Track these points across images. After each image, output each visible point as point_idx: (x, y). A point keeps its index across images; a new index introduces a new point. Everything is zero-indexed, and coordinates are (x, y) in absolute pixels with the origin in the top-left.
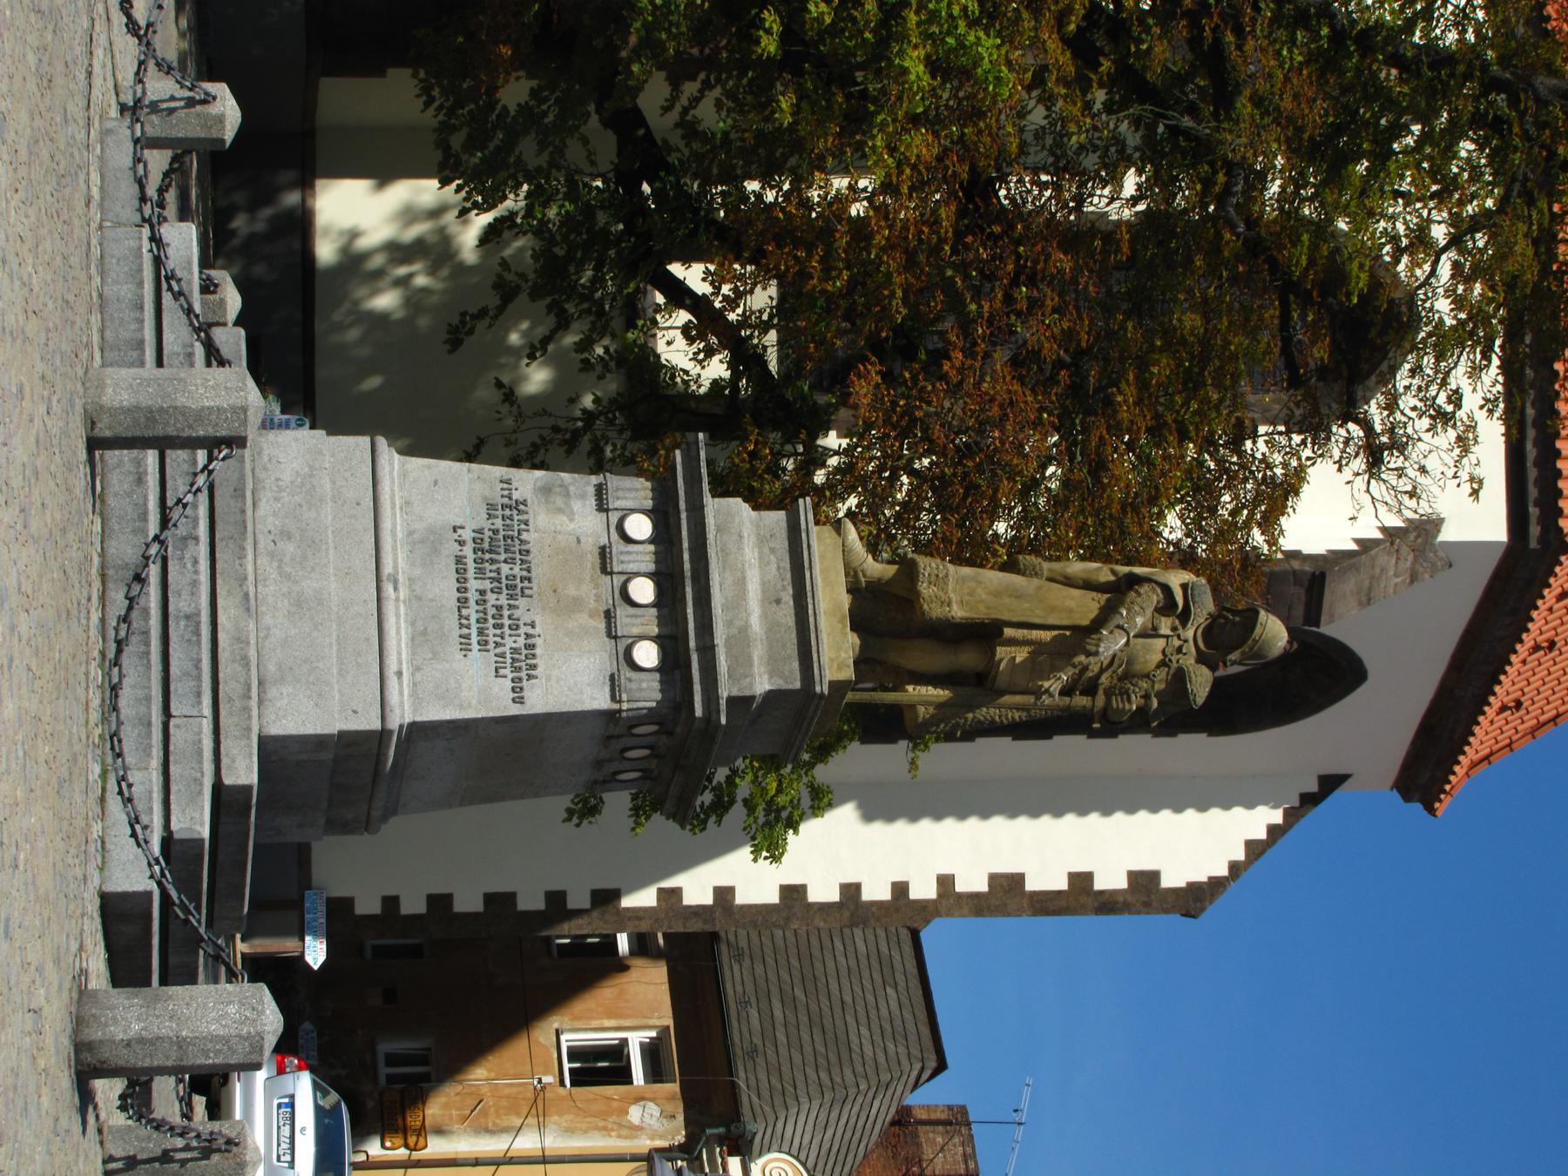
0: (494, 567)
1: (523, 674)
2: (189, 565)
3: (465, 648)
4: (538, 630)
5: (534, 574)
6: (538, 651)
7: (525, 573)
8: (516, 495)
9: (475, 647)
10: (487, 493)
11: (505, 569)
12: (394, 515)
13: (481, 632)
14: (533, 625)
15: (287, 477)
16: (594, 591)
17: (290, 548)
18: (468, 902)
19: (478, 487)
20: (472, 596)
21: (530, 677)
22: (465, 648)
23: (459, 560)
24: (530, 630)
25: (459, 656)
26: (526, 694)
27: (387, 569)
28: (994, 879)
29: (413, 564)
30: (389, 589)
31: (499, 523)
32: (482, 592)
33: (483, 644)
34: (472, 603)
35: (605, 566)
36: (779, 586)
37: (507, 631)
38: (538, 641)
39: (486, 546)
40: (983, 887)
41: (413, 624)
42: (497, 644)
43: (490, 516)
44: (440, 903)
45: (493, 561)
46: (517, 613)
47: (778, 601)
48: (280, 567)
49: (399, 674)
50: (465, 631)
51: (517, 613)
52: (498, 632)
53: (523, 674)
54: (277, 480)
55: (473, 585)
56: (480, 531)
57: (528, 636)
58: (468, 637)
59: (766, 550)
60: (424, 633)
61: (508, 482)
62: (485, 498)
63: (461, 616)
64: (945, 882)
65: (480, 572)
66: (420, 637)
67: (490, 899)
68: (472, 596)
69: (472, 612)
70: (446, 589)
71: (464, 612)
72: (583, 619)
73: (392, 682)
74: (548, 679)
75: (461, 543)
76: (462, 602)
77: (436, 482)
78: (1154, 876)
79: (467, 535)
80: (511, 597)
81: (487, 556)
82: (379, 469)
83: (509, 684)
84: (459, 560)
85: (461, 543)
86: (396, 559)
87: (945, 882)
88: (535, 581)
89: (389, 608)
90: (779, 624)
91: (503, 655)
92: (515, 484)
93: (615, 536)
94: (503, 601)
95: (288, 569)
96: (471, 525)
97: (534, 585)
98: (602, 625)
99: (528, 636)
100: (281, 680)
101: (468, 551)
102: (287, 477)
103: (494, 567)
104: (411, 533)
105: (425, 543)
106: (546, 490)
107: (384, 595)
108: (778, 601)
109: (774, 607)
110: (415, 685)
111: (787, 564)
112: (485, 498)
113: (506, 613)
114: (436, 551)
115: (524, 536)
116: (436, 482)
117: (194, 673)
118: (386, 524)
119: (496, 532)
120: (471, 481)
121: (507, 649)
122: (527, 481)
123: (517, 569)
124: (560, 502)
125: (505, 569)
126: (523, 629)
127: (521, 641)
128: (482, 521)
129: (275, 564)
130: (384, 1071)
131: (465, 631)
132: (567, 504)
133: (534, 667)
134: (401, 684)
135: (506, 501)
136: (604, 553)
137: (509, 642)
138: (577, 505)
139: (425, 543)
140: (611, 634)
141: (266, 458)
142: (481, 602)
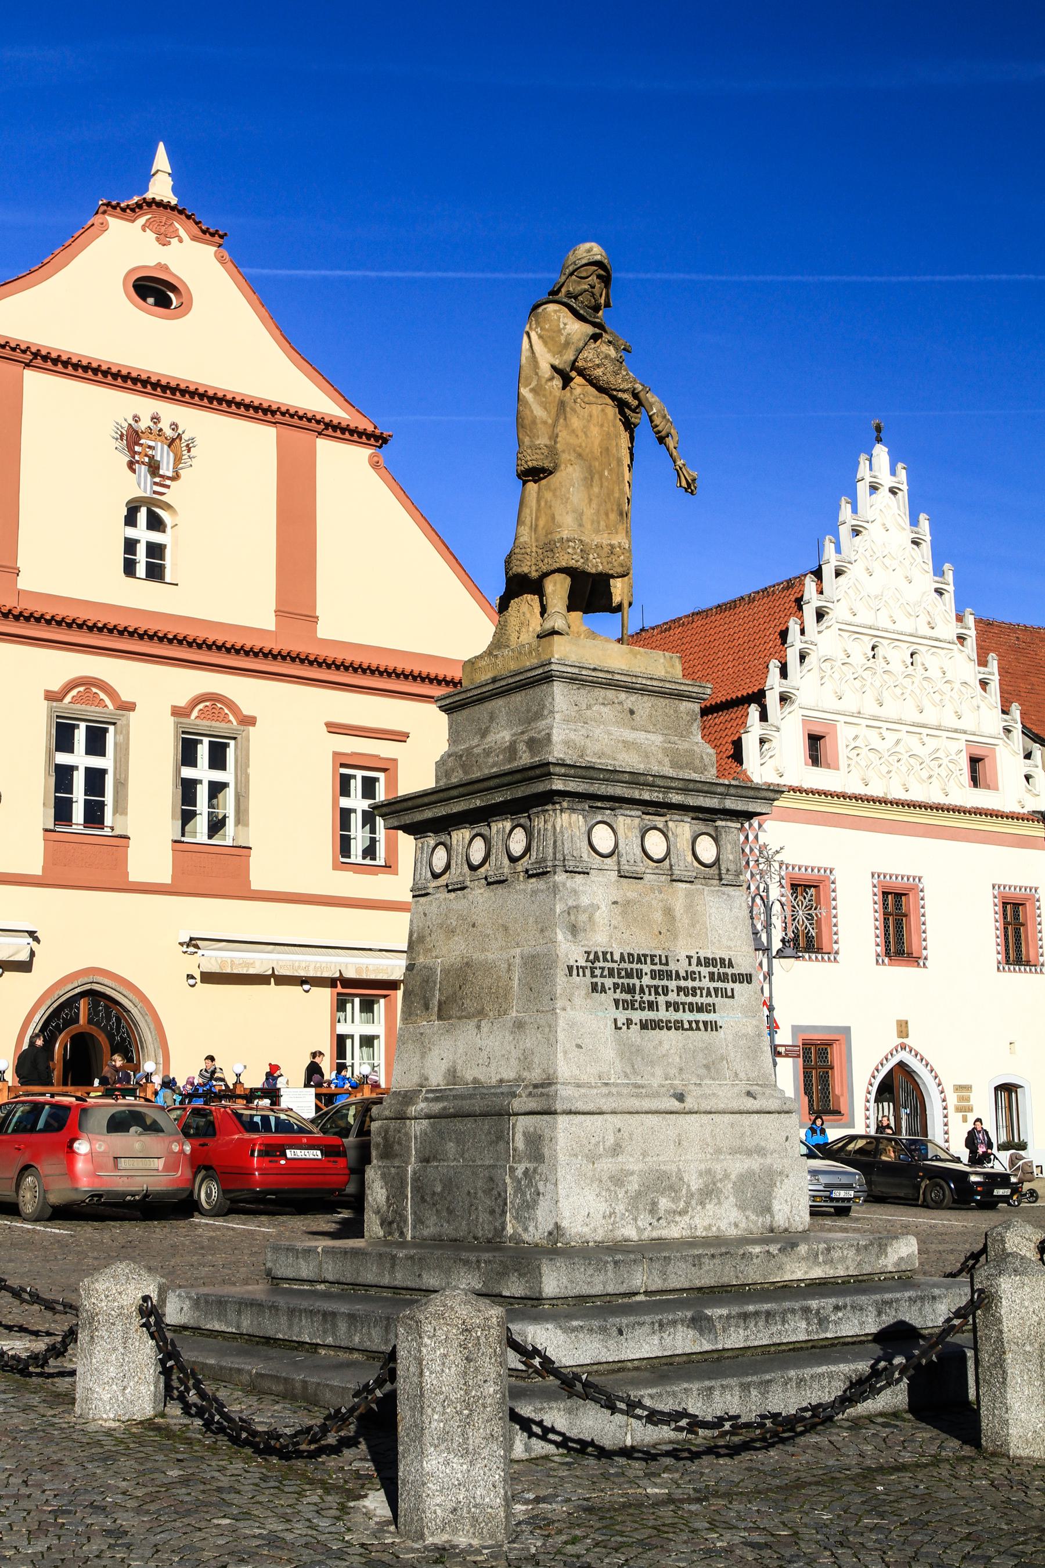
0: (647, 991)
1: (730, 971)
2: (840, 1314)
3: (714, 1026)
4: (693, 953)
11: (646, 980)
13: (700, 1009)
14: (689, 958)
16: (652, 892)
17: (664, 1203)
20: (673, 1016)
21: (731, 965)
22: (714, 1026)
23: (644, 1026)
24: (694, 961)
31: (609, 982)
32: (668, 1005)
33: (710, 1008)
36: (619, 708)
37: (696, 984)
38: (702, 955)
39: (629, 997)
42: (709, 994)
43: (604, 990)
45: (642, 991)
48: (680, 1214)
50: (701, 1025)
51: (682, 974)
53: (730, 971)
54: (604, 1217)
55: (662, 1014)
56: (616, 1002)
58: (705, 1023)
59: (589, 712)
60: (707, 1067)
61: (570, 968)
62: (587, 994)
63: (691, 1029)
65: (652, 1006)
68: (673, 1016)
69: (687, 1017)
71: (686, 1026)
72: (679, 907)
74: (730, 948)
75: (629, 1022)
76: (679, 1025)
77: (579, 1046)
79: (622, 1016)
80: (669, 976)
81: (637, 997)
83: (737, 986)
84: (644, 1026)
91: (716, 990)
92: (572, 963)
94: (672, 984)
95: (682, 1204)
97: (658, 952)
99: (699, 963)
100: (768, 1210)
101: (637, 1016)
102: (603, 1207)
103: (647, 991)
111: (600, 693)
114: (639, 1050)
115: (617, 957)
116: (579, 1046)
119: (616, 986)
121: (712, 985)
123: (646, 968)
124: (583, 917)
125: (646, 980)
127: (705, 971)
129: (678, 1218)
131: (701, 1025)
133: (722, 960)
135: (588, 972)
137: (706, 983)
138: (585, 900)
141: (586, 1229)
142: (676, 1007)
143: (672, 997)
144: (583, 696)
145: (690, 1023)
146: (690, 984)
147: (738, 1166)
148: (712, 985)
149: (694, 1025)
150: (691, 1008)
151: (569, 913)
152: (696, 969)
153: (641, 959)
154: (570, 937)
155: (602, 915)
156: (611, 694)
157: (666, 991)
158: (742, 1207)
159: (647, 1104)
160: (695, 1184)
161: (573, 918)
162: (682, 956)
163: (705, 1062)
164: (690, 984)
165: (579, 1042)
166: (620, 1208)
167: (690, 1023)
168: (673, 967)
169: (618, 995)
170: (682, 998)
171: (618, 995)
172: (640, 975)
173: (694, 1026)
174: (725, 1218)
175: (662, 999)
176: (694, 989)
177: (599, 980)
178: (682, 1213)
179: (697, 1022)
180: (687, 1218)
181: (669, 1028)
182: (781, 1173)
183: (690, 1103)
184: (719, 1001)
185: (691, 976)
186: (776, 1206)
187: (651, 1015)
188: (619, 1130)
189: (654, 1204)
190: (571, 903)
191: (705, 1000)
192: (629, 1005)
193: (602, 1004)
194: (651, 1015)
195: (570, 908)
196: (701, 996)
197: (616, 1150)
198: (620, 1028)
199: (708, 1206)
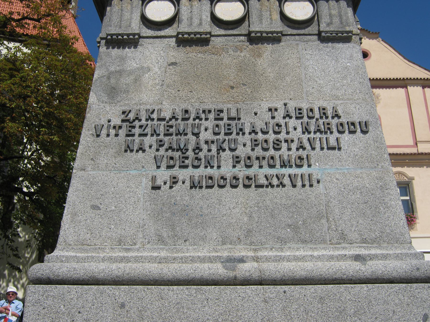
0: (205, 147)
3: (310, 182)
4: (279, 105)
6: (305, 106)
7: (211, 116)
8: (117, 121)
10: (112, 151)
12: (137, 259)
19: (103, 161)
20: (241, 172)
22: (310, 182)
24: (281, 112)
26: (356, 120)
27: (218, 270)
29: (203, 239)
30: (247, 269)
32: (237, 160)
34: (250, 172)
35: (200, 41)
41: (283, 241)
42: (301, 147)
43: (141, 149)
49: (357, 258)
52: (284, 146)
55: (227, 170)
57: (288, 116)
60: (295, 228)
62: (118, 153)
66: (302, 233)
68: (241, 172)
70: (233, 203)
75: (174, 181)
77: (95, 207)
79: (163, 175)
81: (190, 153)
82: (75, 276)
83: (346, 137)
85: (174, 181)
86: (201, 258)
88: (220, 107)
89: (272, 269)
92: (104, 121)
93: (169, 31)
96: (152, 170)
98: (268, 48)
99: (288, 116)
103: (205, 147)
104: (161, 240)
105: (173, 224)
106: (113, 93)
107: (256, 276)
110: (364, 241)
112: (118, 153)
114: (185, 210)
115: (167, 115)
118: (153, 269)
120: (96, 167)
122: (100, 109)
124: (126, 80)
126: (279, 119)
132: (131, 73)
133: (323, 112)
134: (372, 257)
135: (122, 132)
136: (184, 41)
139: (173, 224)
140: (274, 38)
149: (275, 182)
151: (109, 78)
152: (282, 122)
154: (105, 99)
161: (113, 81)
163: (290, 221)
165: (97, 203)
181: (234, 187)
188: (123, 306)
190: (112, 69)
193: (137, 161)
195: (112, 73)
196: (289, 149)
198: (159, 188)
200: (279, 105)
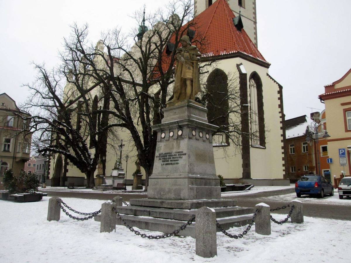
1: (182, 153)
4: (176, 151)
5: (168, 152)
9: (178, 162)
11: (168, 157)
13: (176, 161)
14: (175, 152)
15: (153, 193)
17: (162, 193)
18: (283, 162)
21: (182, 152)
22: (178, 163)
23: (167, 164)
25: (179, 164)
28: (279, 108)
31: (162, 158)
32: (170, 161)
37: (176, 156)
40: (280, 109)
43: (161, 159)
44: (284, 165)
46: (174, 155)
47: (175, 112)
49: (180, 175)
51: (174, 155)
55: (169, 162)
57: (177, 153)
58: (176, 163)
60: (175, 171)
61: (156, 157)
63: (174, 164)
64: (280, 112)
65: (168, 161)
67: (283, 160)
73: (181, 176)
74: (183, 149)
76: (172, 164)
78: (278, 91)
83: (183, 156)
87: (280, 112)
90: (178, 112)
94: (172, 157)
95: (165, 194)
100: (180, 196)
101: (165, 163)
102: (153, 193)
108: (175, 112)
109: (176, 113)
113: (173, 157)
115: (164, 154)
117: (167, 214)
122: (157, 154)
123: (168, 155)
124: (160, 148)
125: (168, 157)
126: (176, 154)
127: (177, 154)
128: (161, 161)
130: (307, 170)
137: (178, 156)
138: (160, 145)
142: (172, 161)
143: (171, 159)
144: (168, 113)
145: (174, 163)
146: (175, 156)
147: (174, 187)
148: (178, 156)
150: (174, 161)
153: (167, 153)
155: (162, 148)
156: (172, 111)
157: (170, 158)
158: (175, 195)
159: (161, 177)
160: (167, 190)
162: (174, 152)
164: (175, 156)
166: (156, 193)
167: (174, 163)
168: (172, 154)
169: (163, 160)
170: (173, 159)
171: (163, 160)
172: (167, 156)
173: (174, 164)
174: (172, 196)
175: (170, 160)
176: (175, 157)
177: (160, 158)
178: (165, 195)
179: (175, 163)
180: (166, 196)
182: (182, 189)
183: (168, 177)
184: (179, 159)
185: (175, 155)
186: (181, 195)
187: (167, 163)
189: (161, 193)
191: (177, 159)
192: (164, 161)
194: (167, 163)
197: (156, 185)
199: (169, 194)
200: (176, 151)
